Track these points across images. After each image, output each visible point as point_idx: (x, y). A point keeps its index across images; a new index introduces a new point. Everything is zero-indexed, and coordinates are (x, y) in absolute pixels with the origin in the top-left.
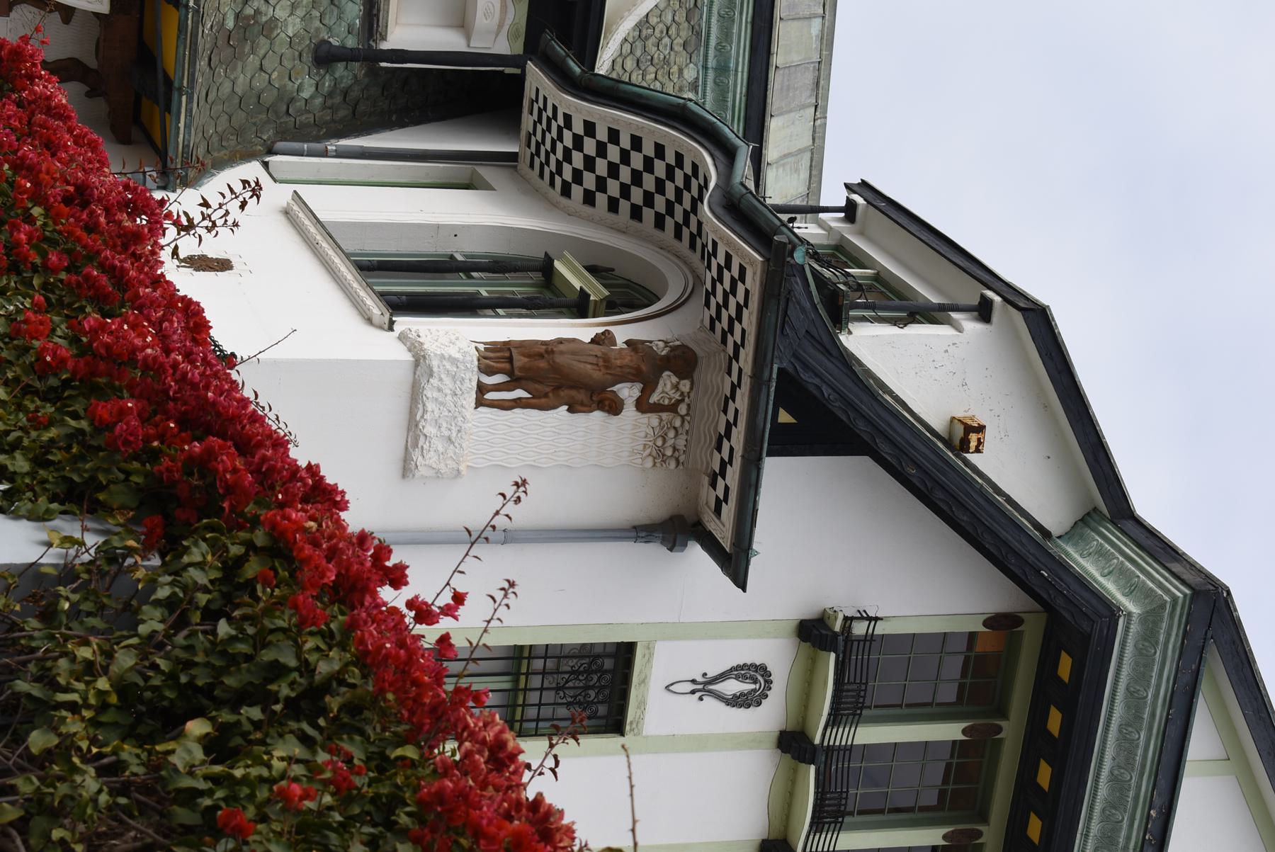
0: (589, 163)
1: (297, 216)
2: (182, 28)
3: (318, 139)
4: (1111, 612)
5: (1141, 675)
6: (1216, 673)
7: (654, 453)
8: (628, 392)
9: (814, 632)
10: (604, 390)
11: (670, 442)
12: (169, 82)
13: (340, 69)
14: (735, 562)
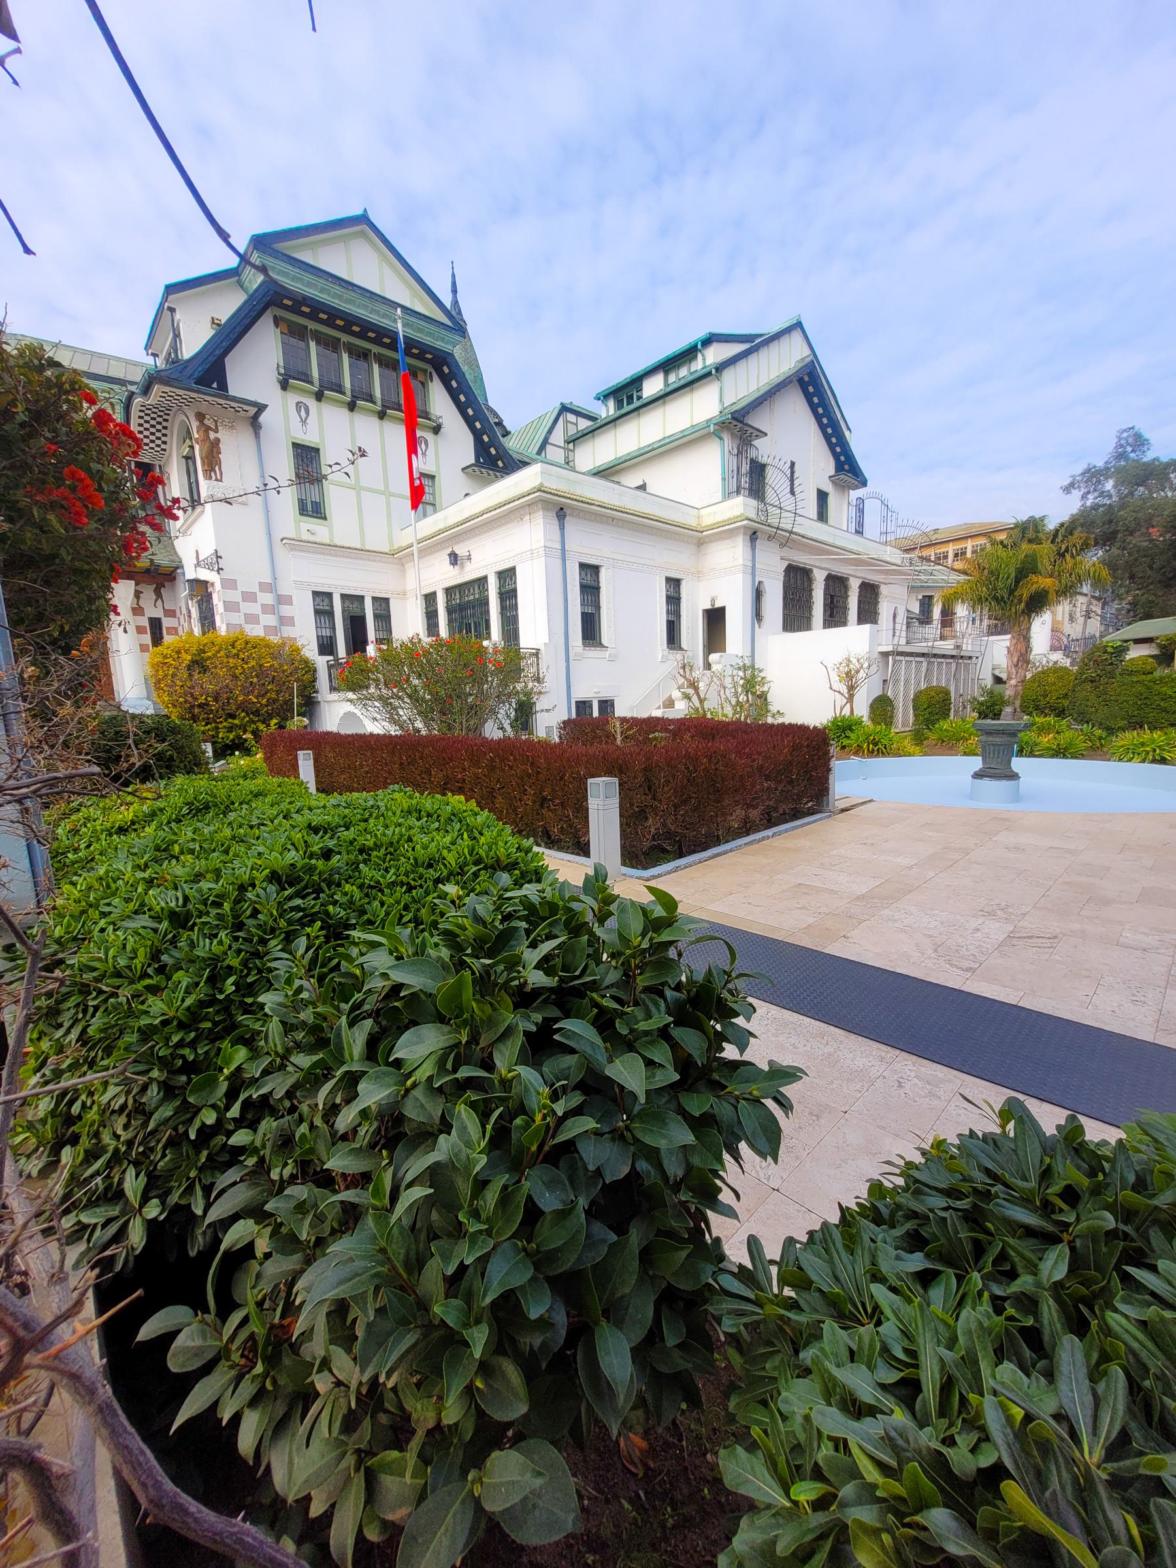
6: (281, 246)
9: (284, 386)
14: (261, 408)
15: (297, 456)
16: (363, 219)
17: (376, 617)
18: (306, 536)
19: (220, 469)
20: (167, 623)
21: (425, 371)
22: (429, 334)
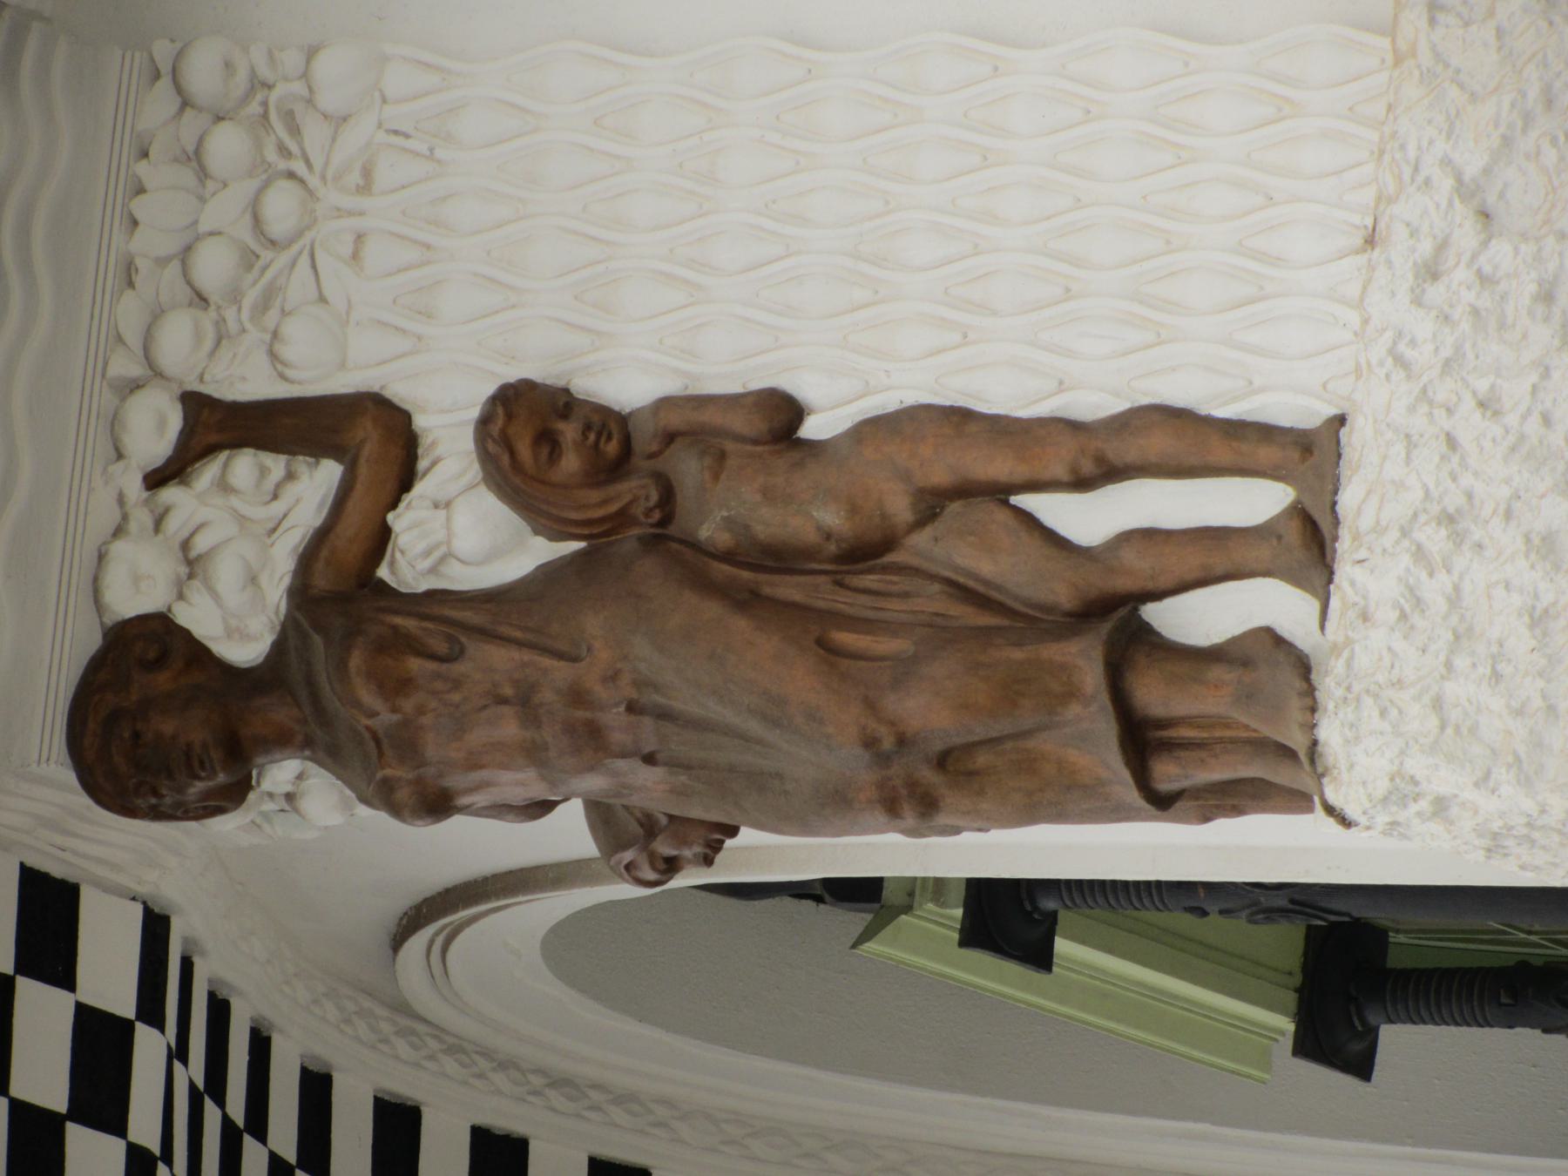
7: (314, 133)
8: (462, 535)
10: (602, 533)
11: (225, 209)
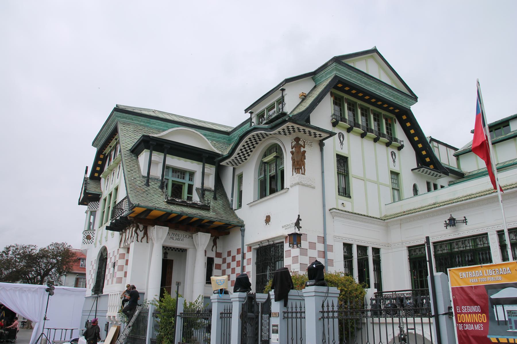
0: (244, 155)
1: (251, 205)
2: (220, 221)
3: (228, 201)
4: (336, 77)
5: (345, 73)
6: (345, 61)
8: (302, 149)
9: (334, 124)
12: (226, 224)
13: (217, 196)
15: (338, 161)
16: (375, 50)
17: (374, 261)
18: (341, 208)
19: (304, 168)
20: (217, 261)
21: (391, 118)
22: (402, 100)
